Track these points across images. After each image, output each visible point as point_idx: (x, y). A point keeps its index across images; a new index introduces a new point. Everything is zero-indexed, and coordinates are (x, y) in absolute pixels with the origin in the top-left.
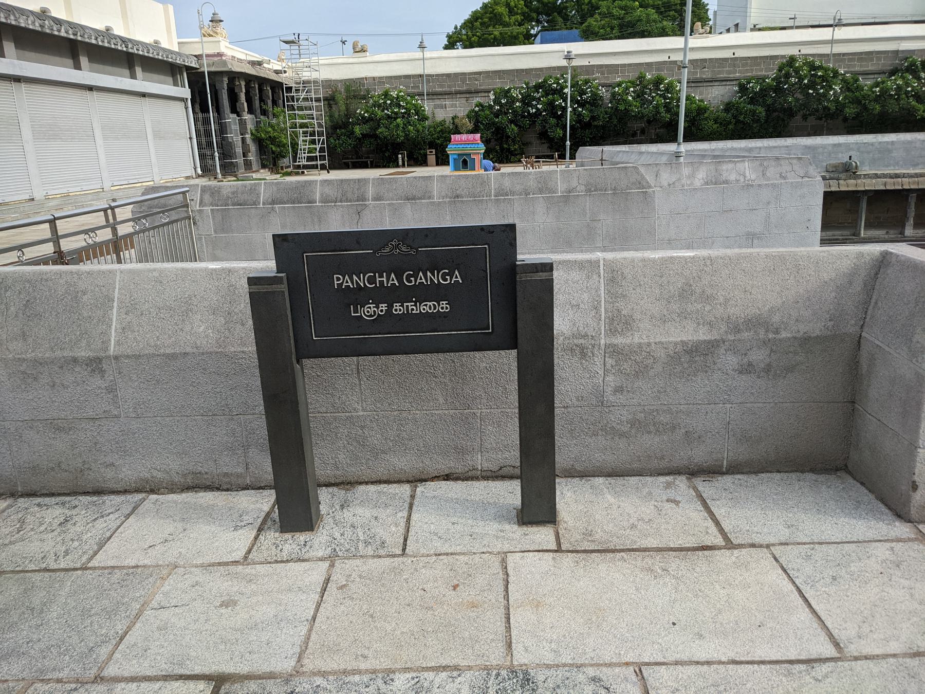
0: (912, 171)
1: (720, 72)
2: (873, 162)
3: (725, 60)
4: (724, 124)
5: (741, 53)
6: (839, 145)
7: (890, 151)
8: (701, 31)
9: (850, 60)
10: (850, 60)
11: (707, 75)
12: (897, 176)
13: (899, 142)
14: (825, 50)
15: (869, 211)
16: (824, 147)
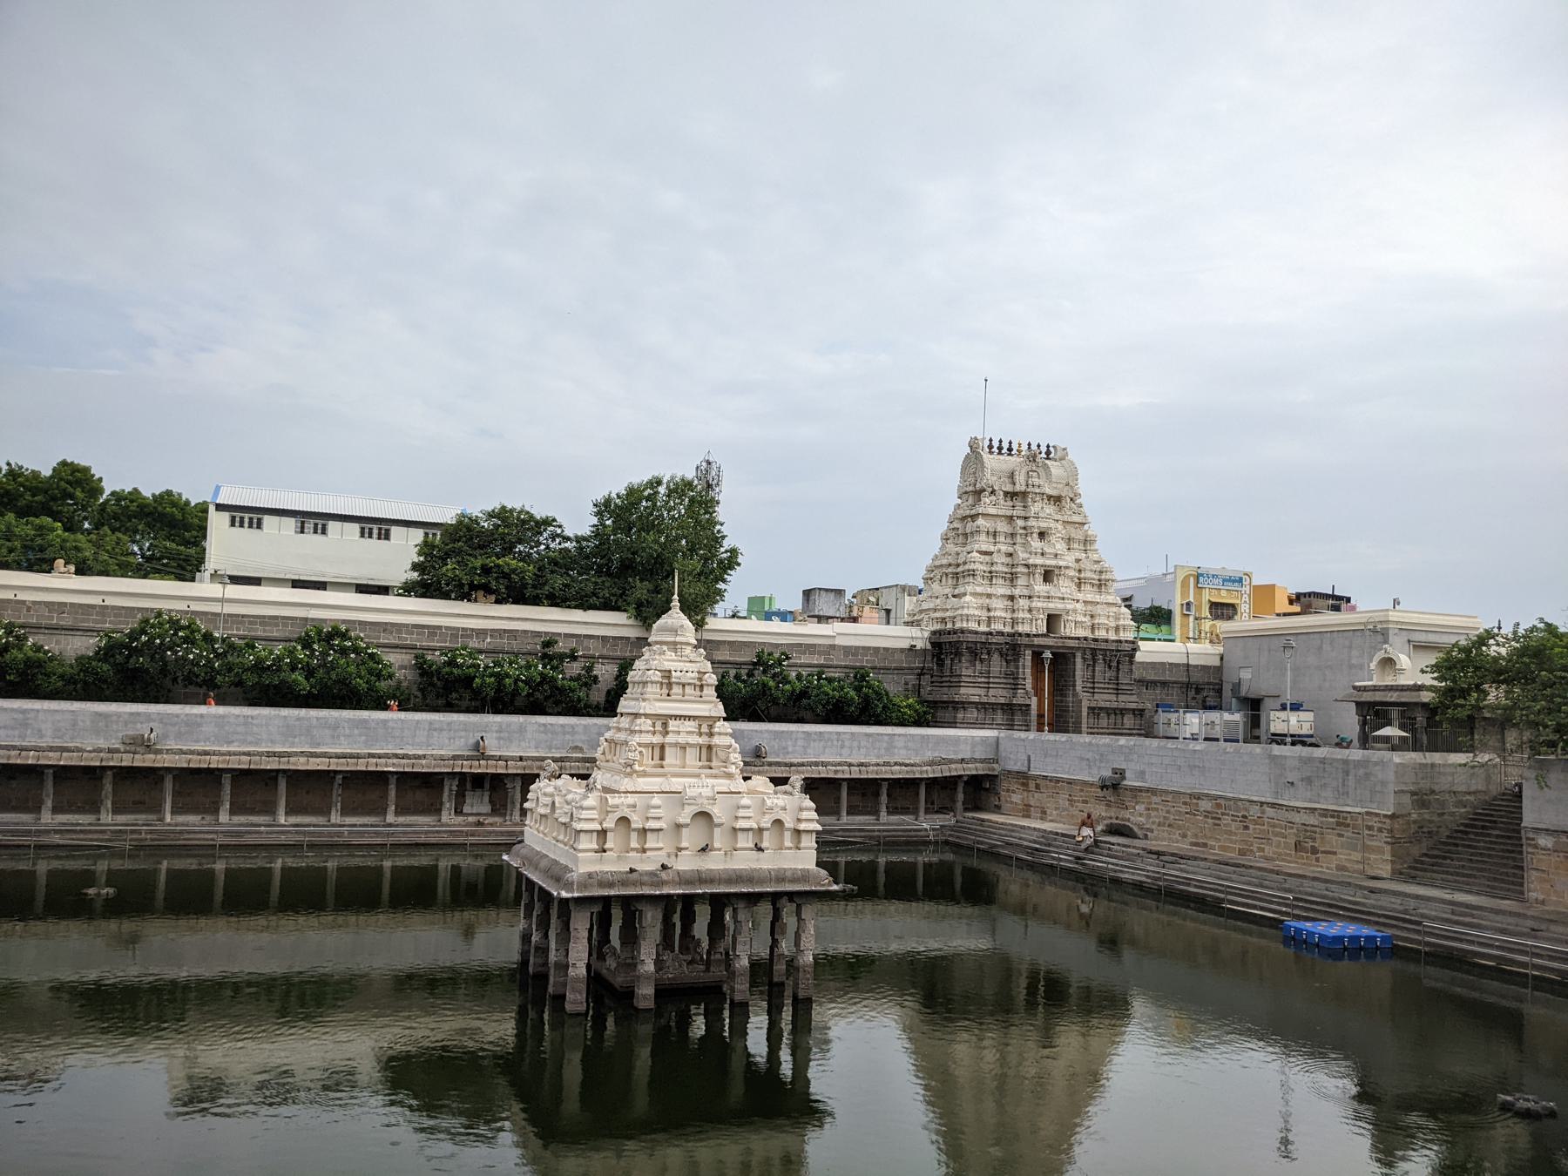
0: (224, 749)
1: (84, 621)
2: (179, 736)
3: (93, 606)
4: (69, 680)
6: (138, 714)
7: (200, 725)
8: (62, 569)
9: (251, 623)
10: (251, 623)
11: (67, 621)
12: (206, 753)
13: (209, 715)
14: (216, 608)
15: (176, 794)
16: (119, 715)
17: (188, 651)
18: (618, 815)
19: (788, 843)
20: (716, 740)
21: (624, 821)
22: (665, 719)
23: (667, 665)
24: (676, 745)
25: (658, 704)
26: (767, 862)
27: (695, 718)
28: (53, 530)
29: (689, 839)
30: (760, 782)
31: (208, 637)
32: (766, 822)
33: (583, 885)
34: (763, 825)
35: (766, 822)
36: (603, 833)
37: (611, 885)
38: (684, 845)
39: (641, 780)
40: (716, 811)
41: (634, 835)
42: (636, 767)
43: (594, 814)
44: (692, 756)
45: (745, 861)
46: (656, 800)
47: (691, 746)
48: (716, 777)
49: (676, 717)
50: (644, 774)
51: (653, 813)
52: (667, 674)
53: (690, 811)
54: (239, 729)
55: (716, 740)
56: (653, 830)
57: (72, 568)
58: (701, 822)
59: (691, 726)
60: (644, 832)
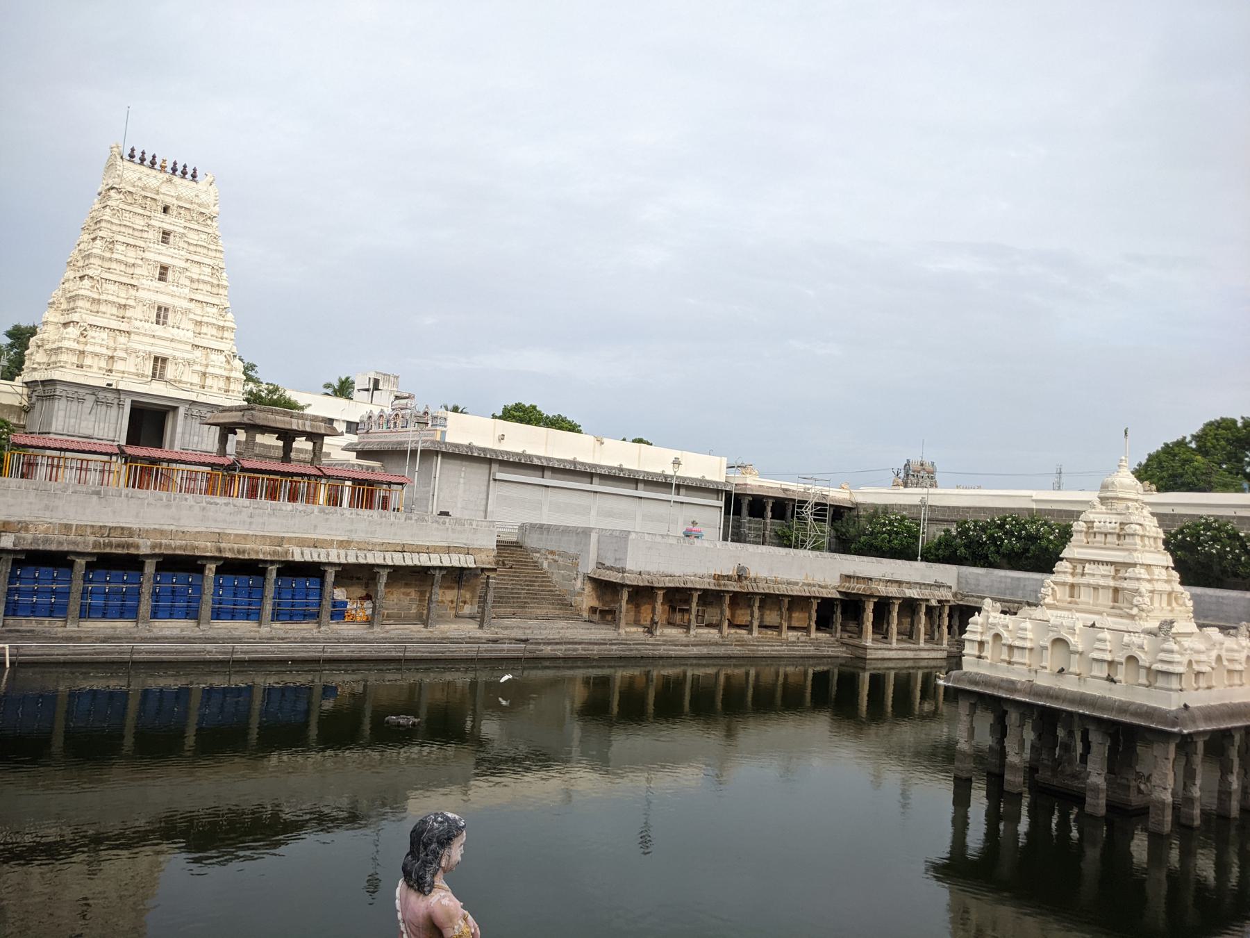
5: (1179, 511)
17: (1212, 547)
18: (993, 632)
19: (1143, 680)
20: (1125, 584)
21: (997, 637)
22: (1083, 562)
23: (1091, 517)
24: (1088, 585)
25: (1076, 550)
26: (1117, 694)
27: (1112, 563)
28: (1192, 461)
29: (1051, 661)
30: (1214, 633)
31: (1234, 536)
32: (1120, 657)
33: (958, 680)
34: (1117, 659)
35: (1120, 657)
36: (981, 643)
37: (976, 683)
38: (1044, 664)
39: (1048, 612)
40: (1076, 642)
41: (1005, 650)
42: (1048, 600)
43: (979, 629)
44: (1105, 598)
45: (1096, 688)
46: (1028, 624)
47: (1103, 587)
48: (1122, 617)
49: (1090, 561)
50: (1057, 608)
51: (1021, 634)
52: (1090, 524)
53: (1053, 635)
54: (1213, 607)
55: (1125, 584)
56: (1018, 648)
57: (1154, 487)
58: (1060, 649)
59: (1103, 569)
60: (1011, 647)
